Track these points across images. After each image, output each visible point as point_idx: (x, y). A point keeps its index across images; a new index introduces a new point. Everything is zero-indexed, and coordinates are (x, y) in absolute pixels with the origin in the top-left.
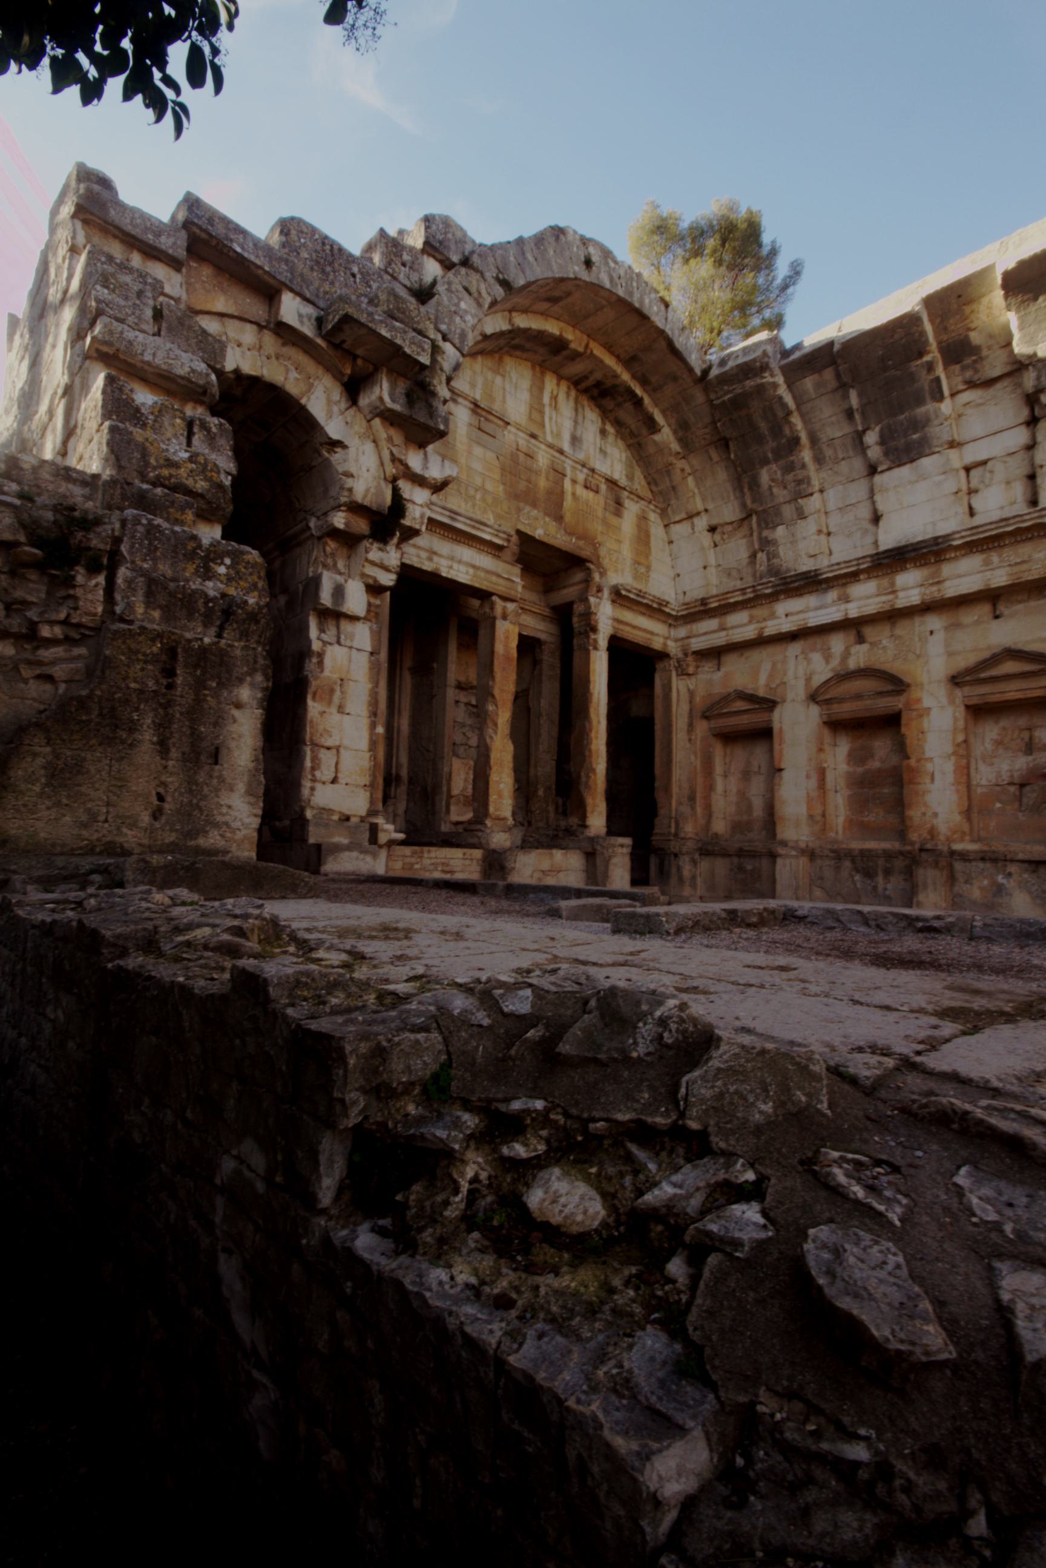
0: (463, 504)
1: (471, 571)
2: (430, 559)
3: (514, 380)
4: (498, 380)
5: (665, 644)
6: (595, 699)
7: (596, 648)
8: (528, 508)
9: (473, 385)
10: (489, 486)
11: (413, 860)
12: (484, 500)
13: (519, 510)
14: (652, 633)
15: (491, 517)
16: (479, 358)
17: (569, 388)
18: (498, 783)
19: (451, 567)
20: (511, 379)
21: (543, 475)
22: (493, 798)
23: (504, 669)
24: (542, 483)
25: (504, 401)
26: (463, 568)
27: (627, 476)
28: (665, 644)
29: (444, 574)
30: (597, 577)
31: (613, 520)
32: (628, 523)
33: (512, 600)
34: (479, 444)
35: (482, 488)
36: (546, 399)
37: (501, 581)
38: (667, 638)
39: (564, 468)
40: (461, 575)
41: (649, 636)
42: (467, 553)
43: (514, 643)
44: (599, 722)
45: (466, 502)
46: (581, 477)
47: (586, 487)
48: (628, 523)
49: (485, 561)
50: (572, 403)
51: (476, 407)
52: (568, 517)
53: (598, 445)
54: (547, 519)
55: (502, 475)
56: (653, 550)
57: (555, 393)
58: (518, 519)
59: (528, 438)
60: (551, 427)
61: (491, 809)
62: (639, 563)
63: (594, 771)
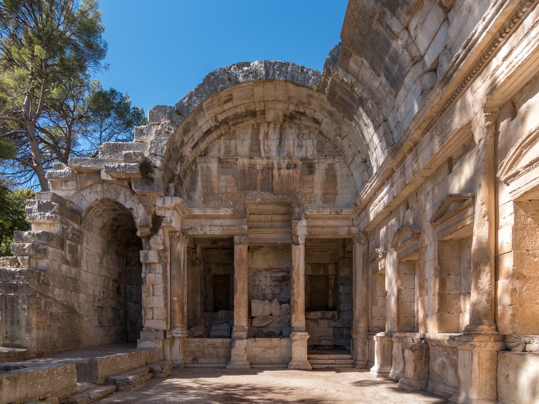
0: (216, 203)
1: (221, 229)
2: (202, 230)
3: (241, 138)
4: (233, 142)
5: (349, 231)
6: (296, 268)
7: (297, 244)
8: (251, 192)
9: (219, 151)
10: (229, 190)
11: (199, 343)
12: (227, 197)
13: (245, 194)
14: (338, 227)
15: (231, 203)
16: (222, 138)
17: (275, 124)
18: (239, 312)
19: (211, 230)
20: (239, 137)
21: (260, 174)
22: (236, 318)
23: (239, 265)
24: (259, 177)
25: (236, 149)
26: (216, 229)
27: (318, 151)
28: (349, 231)
29: (208, 234)
30: (297, 210)
31: (309, 178)
32: (319, 176)
33: (243, 235)
34: (223, 174)
35: (226, 192)
36: (261, 137)
37: (236, 228)
38: (350, 226)
39: (273, 164)
40: (216, 232)
41: (335, 229)
42: (218, 222)
43: (245, 253)
44: (299, 279)
45: (218, 201)
46: (284, 165)
47: (288, 168)
48: (319, 176)
49: (229, 222)
50: (278, 131)
51: (220, 160)
52: (276, 187)
53: (296, 144)
54: (262, 193)
55: (236, 183)
56: (339, 183)
57: (266, 131)
58: (246, 198)
59: (249, 160)
60: (264, 149)
61: (235, 323)
62: (327, 194)
63: (296, 302)
